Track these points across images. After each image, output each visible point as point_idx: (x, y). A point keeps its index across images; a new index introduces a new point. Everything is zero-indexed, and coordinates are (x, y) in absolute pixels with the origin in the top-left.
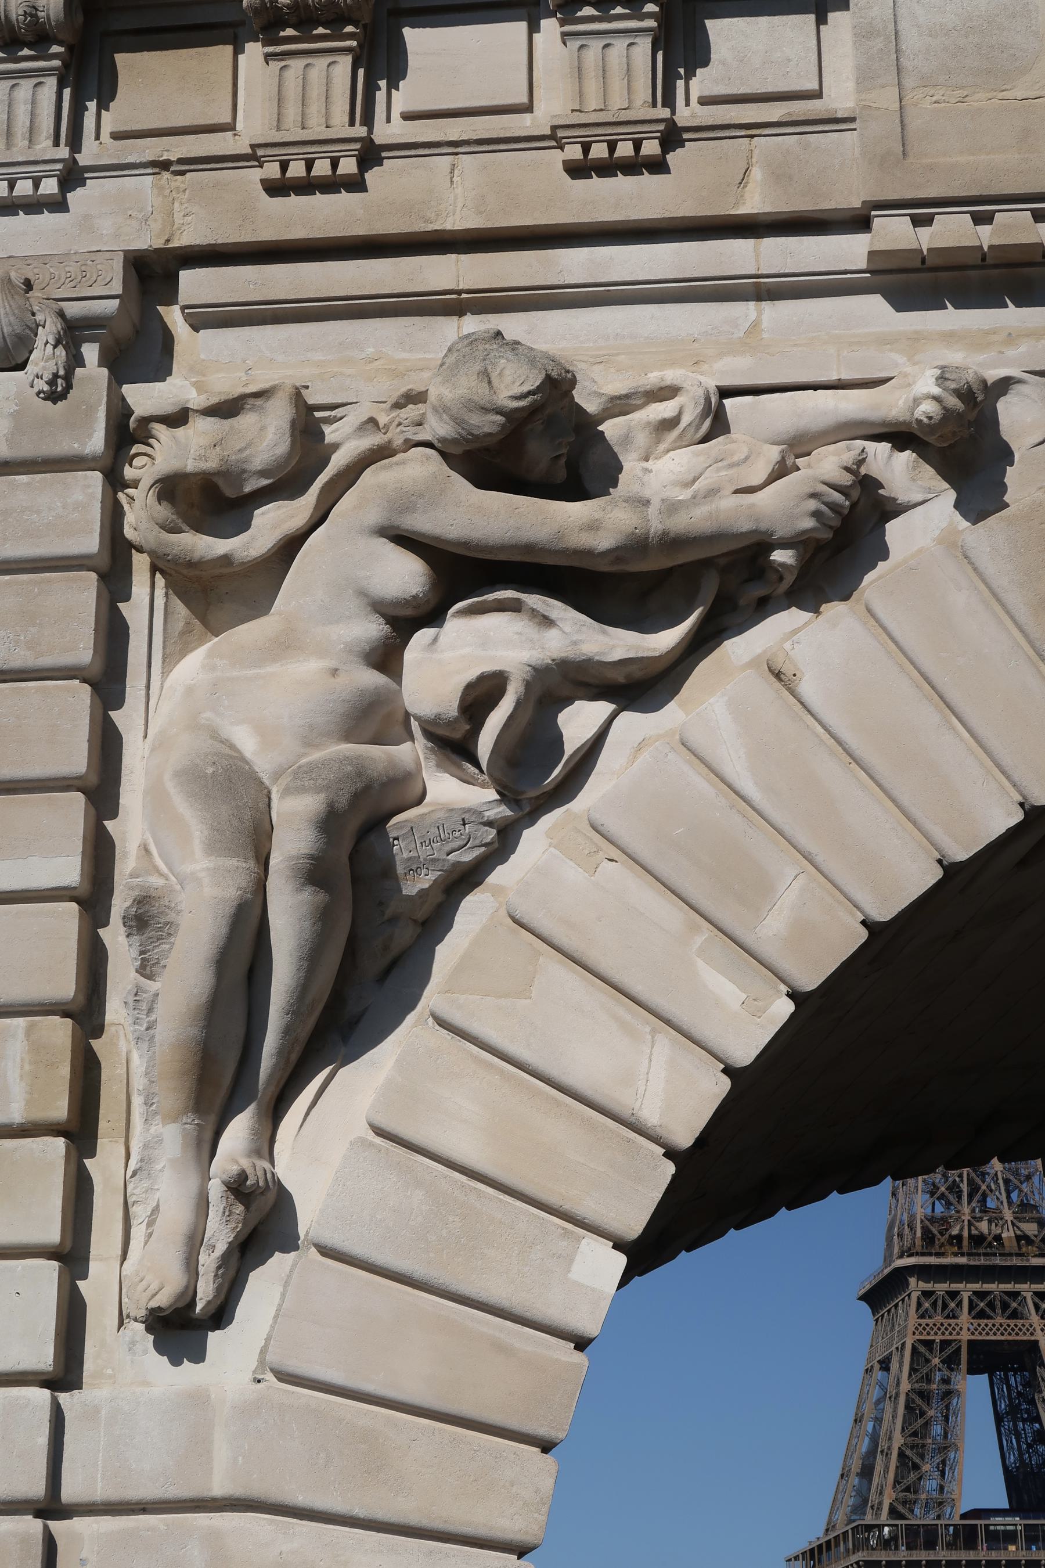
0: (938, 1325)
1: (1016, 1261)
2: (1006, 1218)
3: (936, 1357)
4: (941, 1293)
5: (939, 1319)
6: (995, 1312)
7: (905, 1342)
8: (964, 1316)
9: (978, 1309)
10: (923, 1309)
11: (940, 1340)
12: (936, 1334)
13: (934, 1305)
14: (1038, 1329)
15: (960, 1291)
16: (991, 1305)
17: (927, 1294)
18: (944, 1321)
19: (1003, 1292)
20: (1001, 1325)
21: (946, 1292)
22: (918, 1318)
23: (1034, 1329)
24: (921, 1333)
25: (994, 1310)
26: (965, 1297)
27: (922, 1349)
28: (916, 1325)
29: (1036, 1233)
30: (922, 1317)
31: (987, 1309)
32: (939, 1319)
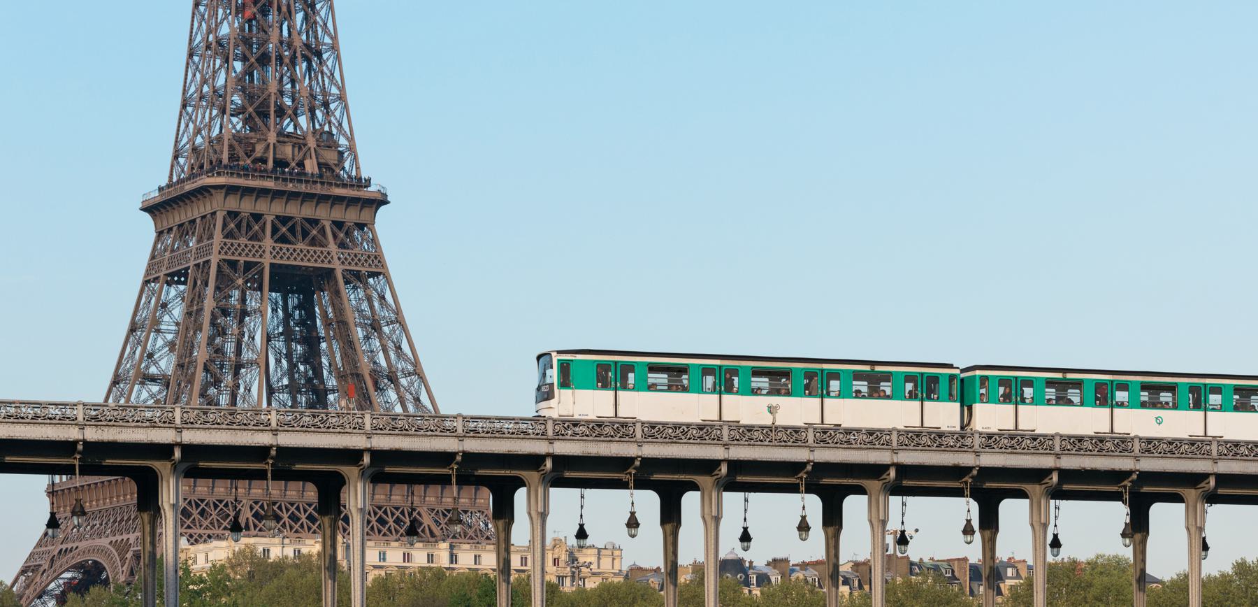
0: (243, 246)
1: (318, 189)
2: (309, 145)
4: (246, 214)
5: (243, 240)
8: (268, 242)
11: (245, 261)
12: (240, 254)
13: (239, 226)
14: (336, 257)
15: (263, 215)
16: (292, 230)
17: (232, 214)
18: (248, 243)
19: (303, 218)
20: (301, 251)
21: (251, 214)
22: (224, 238)
23: (332, 258)
25: (294, 235)
26: (269, 219)
27: (227, 269)
28: (222, 245)
29: (336, 162)
30: (226, 237)
31: (288, 234)
32: (243, 240)
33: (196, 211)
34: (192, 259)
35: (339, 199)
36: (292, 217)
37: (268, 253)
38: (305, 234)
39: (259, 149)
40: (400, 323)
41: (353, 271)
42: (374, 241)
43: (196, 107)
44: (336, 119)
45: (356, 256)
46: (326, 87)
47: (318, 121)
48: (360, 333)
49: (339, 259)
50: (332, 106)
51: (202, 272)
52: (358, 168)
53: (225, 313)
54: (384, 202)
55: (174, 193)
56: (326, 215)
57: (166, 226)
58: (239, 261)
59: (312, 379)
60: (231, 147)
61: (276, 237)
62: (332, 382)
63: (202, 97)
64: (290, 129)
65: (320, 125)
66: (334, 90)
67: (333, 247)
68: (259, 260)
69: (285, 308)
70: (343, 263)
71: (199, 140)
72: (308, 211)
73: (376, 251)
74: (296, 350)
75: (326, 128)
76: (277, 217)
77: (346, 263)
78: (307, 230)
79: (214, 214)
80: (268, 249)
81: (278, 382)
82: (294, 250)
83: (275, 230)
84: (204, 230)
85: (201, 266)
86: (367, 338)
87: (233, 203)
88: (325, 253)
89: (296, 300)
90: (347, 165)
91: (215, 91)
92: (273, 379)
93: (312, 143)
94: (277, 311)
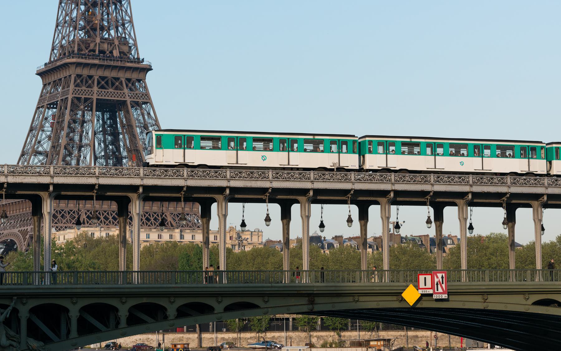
0: (83, 91)
1: (119, 64)
3: (82, 105)
4: (85, 76)
5: (84, 88)
6: (108, 86)
7: (68, 97)
8: (95, 89)
9: (101, 84)
10: (77, 82)
12: (82, 94)
13: (82, 81)
14: (127, 95)
15: (93, 76)
16: (107, 83)
17: (79, 76)
19: (112, 77)
21: (88, 76)
23: (125, 95)
24: (76, 94)
25: (108, 84)
26: (96, 78)
28: (74, 90)
29: (128, 51)
30: (76, 86)
31: (105, 85)
32: (84, 88)
33: (62, 75)
34: (60, 97)
35: (129, 68)
36: (107, 77)
37: (95, 93)
38: (113, 84)
39: (92, 46)
40: (157, 126)
41: (136, 101)
42: (146, 87)
43: (63, 27)
44: (128, 31)
45: (136, 94)
46: (124, 16)
47: (120, 32)
48: (138, 130)
49: (129, 96)
50: (126, 25)
51: (64, 103)
52: (138, 54)
53: (75, 122)
54: (151, 69)
55: (51, 66)
56: (122, 75)
57: (48, 82)
58: (81, 97)
59: (116, 152)
60: (79, 45)
61: (99, 86)
62: (125, 154)
63: (65, 22)
64: (107, 36)
65: (121, 34)
66: (127, 18)
67: (126, 91)
68: (91, 97)
69: (103, 119)
70: (131, 98)
71: (64, 42)
72: (114, 74)
73: (146, 92)
74: (108, 139)
75: (123, 36)
76: (100, 77)
77: (132, 98)
78: (114, 83)
79: (70, 76)
80: (95, 92)
81: (99, 154)
82: (108, 92)
83: (99, 83)
84: (65, 83)
85: (64, 100)
86: (142, 133)
87: (79, 71)
88: (122, 93)
89: (108, 116)
90: (133, 52)
91: (72, 19)
92: (97, 153)
93: (116, 42)
94: (99, 121)
